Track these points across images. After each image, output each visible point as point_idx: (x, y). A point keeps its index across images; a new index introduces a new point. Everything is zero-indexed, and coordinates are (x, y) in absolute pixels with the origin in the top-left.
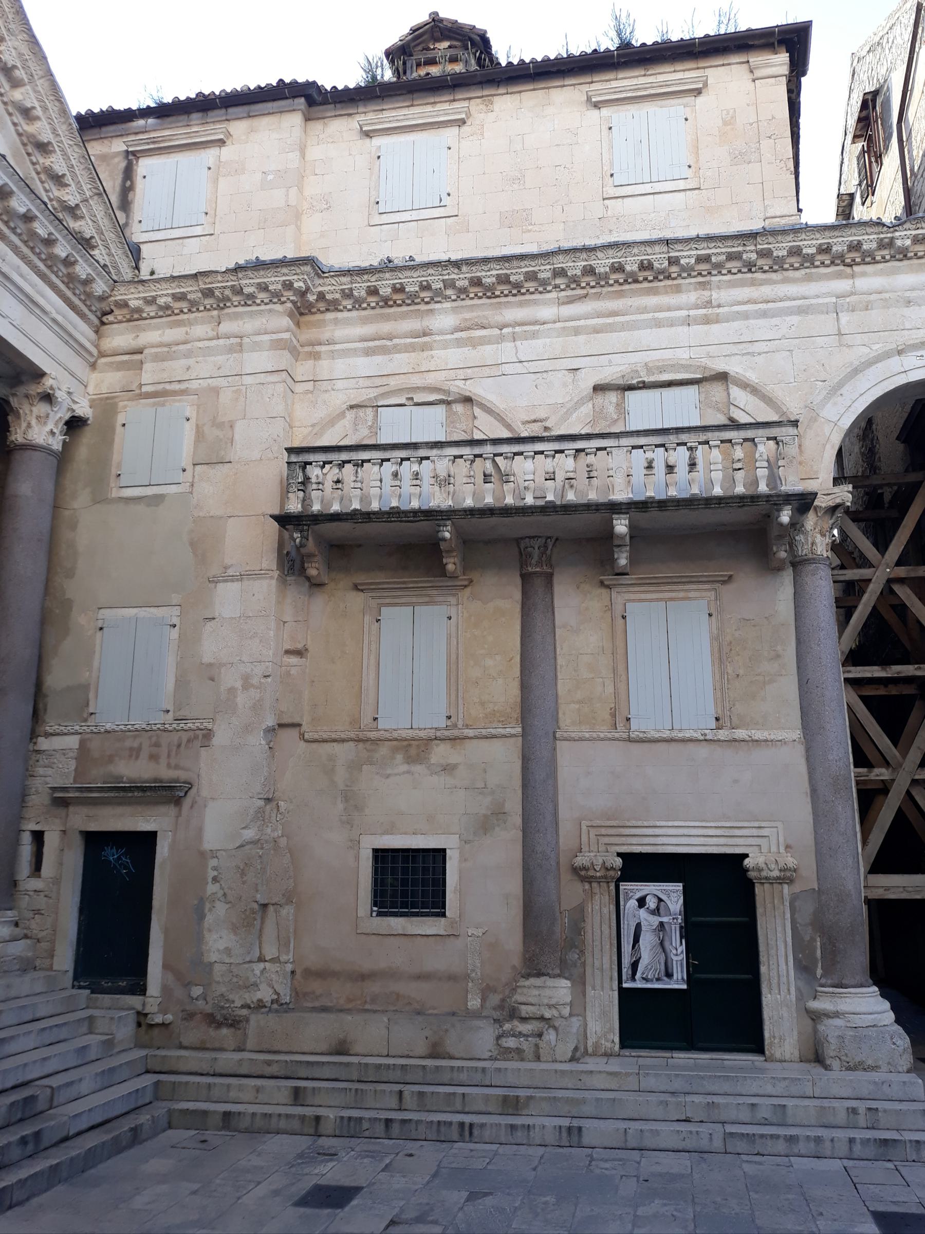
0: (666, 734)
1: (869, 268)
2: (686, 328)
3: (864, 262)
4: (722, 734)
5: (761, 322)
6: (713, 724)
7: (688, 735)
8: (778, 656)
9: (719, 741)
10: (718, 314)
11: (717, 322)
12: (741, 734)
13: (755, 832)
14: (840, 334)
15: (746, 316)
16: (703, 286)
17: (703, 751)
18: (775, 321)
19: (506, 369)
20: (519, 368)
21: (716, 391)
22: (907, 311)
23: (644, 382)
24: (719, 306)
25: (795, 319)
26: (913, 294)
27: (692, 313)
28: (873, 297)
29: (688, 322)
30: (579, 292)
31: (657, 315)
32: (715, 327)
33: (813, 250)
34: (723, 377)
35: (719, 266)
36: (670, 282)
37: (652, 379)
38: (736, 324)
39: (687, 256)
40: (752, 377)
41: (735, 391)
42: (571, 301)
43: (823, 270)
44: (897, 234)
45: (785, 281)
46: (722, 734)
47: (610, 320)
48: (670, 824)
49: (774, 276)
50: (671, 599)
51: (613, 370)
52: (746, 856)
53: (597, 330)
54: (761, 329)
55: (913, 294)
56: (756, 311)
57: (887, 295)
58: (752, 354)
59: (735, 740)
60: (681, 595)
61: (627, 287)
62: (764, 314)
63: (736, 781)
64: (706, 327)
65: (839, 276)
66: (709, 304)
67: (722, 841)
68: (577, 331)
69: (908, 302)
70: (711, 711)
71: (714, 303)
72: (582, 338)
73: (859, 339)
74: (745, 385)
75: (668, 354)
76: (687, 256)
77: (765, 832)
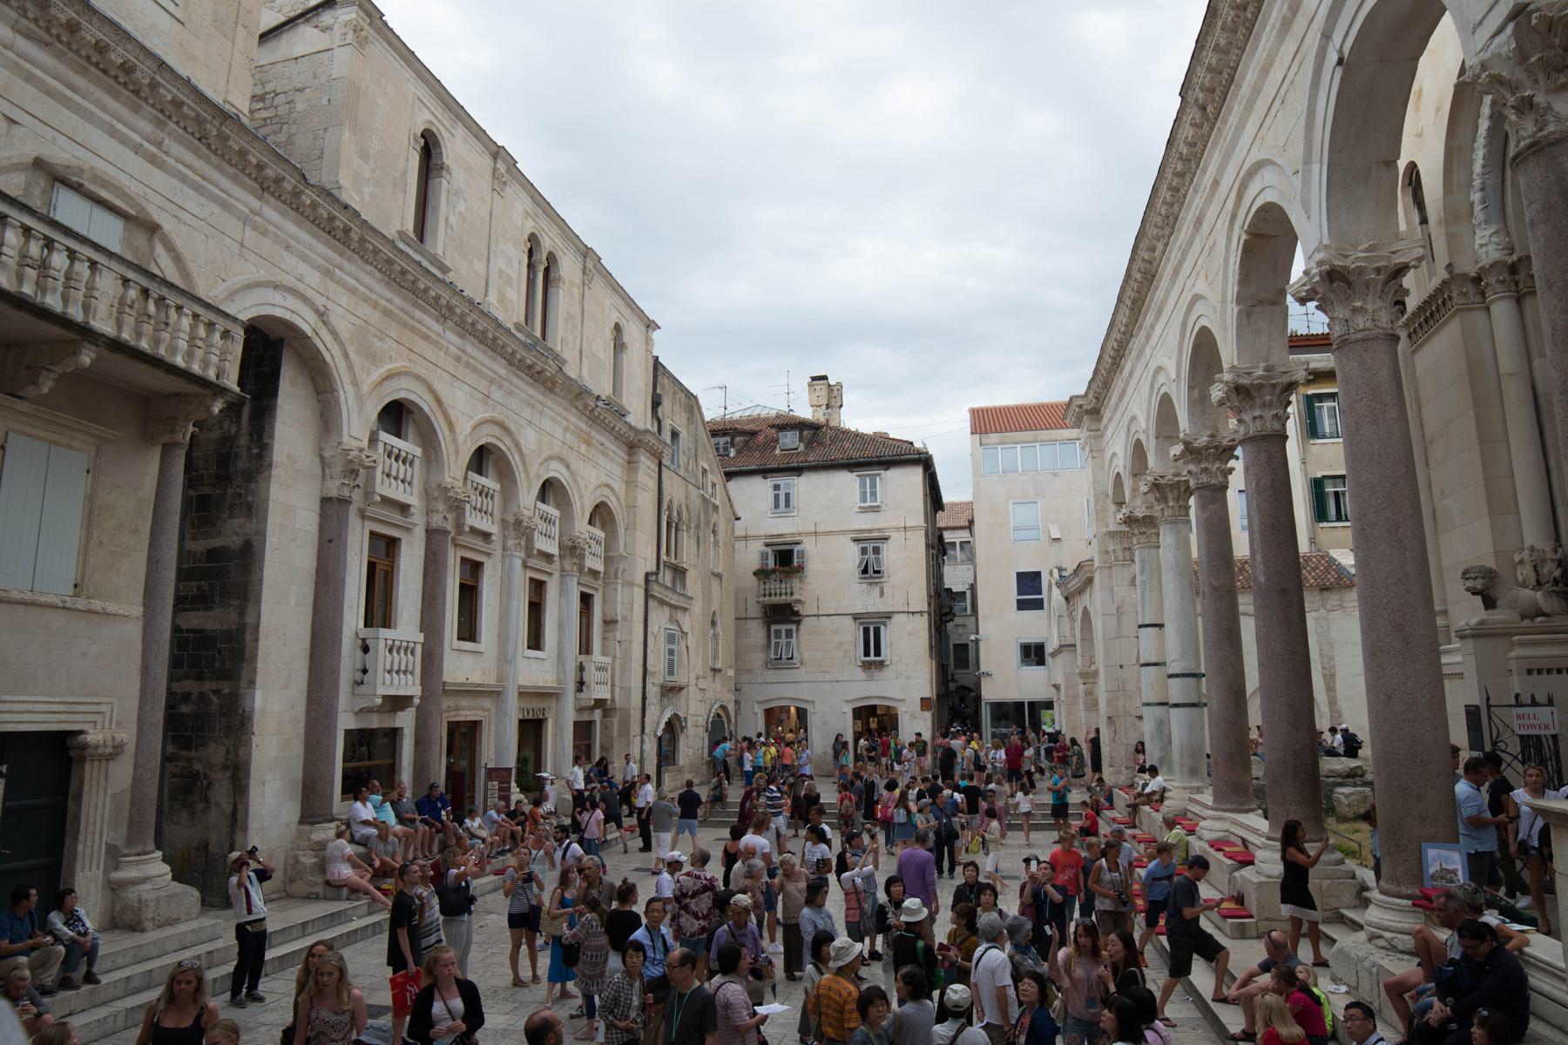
0: (28, 596)
1: (272, 201)
2: (132, 155)
3: (272, 194)
4: (81, 603)
5: (192, 193)
6: (71, 591)
7: (50, 599)
8: (137, 530)
9: (77, 610)
11: (160, 168)
12: (97, 605)
13: (94, 708)
14: (242, 245)
15: (183, 179)
16: (159, 124)
17: (59, 620)
18: (202, 200)
21: (140, 239)
22: (285, 254)
23: (81, 185)
25: (217, 209)
26: (294, 243)
27: (146, 144)
28: (271, 228)
29: (137, 149)
30: (43, 34)
31: (115, 122)
33: (254, 161)
34: (153, 229)
35: (185, 117)
36: (133, 97)
37: (92, 187)
38: (174, 182)
39: (168, 92)
40: (178, 242)
41: (159, 250)
42: (28, 35)
45: (219, 168)
46: (81, 603)
47: (69, 93)
48: (16, 698)
49: (213, 157)
50: (55, 443)
51: (61, 154)
52: (81, 732)
53: (49, 92)
54: (192, 201)
55: (294, 243)
59: (90, 611)
60: (65, 440)
61: (93, 69)
62: (198, 189)
63: (85, 654)
64: (149, 166)
65: (252, 192)
66: (159, 145)
67: (63, 717)
68: (29, 78)
69: (287, 247)
70: (71, 577)
71: (164, 148)
72: (31, 90)
73: (252, 257)
74: (171, 248)
75: (112, 171)
76: (168, 92)
77: (103, 708)
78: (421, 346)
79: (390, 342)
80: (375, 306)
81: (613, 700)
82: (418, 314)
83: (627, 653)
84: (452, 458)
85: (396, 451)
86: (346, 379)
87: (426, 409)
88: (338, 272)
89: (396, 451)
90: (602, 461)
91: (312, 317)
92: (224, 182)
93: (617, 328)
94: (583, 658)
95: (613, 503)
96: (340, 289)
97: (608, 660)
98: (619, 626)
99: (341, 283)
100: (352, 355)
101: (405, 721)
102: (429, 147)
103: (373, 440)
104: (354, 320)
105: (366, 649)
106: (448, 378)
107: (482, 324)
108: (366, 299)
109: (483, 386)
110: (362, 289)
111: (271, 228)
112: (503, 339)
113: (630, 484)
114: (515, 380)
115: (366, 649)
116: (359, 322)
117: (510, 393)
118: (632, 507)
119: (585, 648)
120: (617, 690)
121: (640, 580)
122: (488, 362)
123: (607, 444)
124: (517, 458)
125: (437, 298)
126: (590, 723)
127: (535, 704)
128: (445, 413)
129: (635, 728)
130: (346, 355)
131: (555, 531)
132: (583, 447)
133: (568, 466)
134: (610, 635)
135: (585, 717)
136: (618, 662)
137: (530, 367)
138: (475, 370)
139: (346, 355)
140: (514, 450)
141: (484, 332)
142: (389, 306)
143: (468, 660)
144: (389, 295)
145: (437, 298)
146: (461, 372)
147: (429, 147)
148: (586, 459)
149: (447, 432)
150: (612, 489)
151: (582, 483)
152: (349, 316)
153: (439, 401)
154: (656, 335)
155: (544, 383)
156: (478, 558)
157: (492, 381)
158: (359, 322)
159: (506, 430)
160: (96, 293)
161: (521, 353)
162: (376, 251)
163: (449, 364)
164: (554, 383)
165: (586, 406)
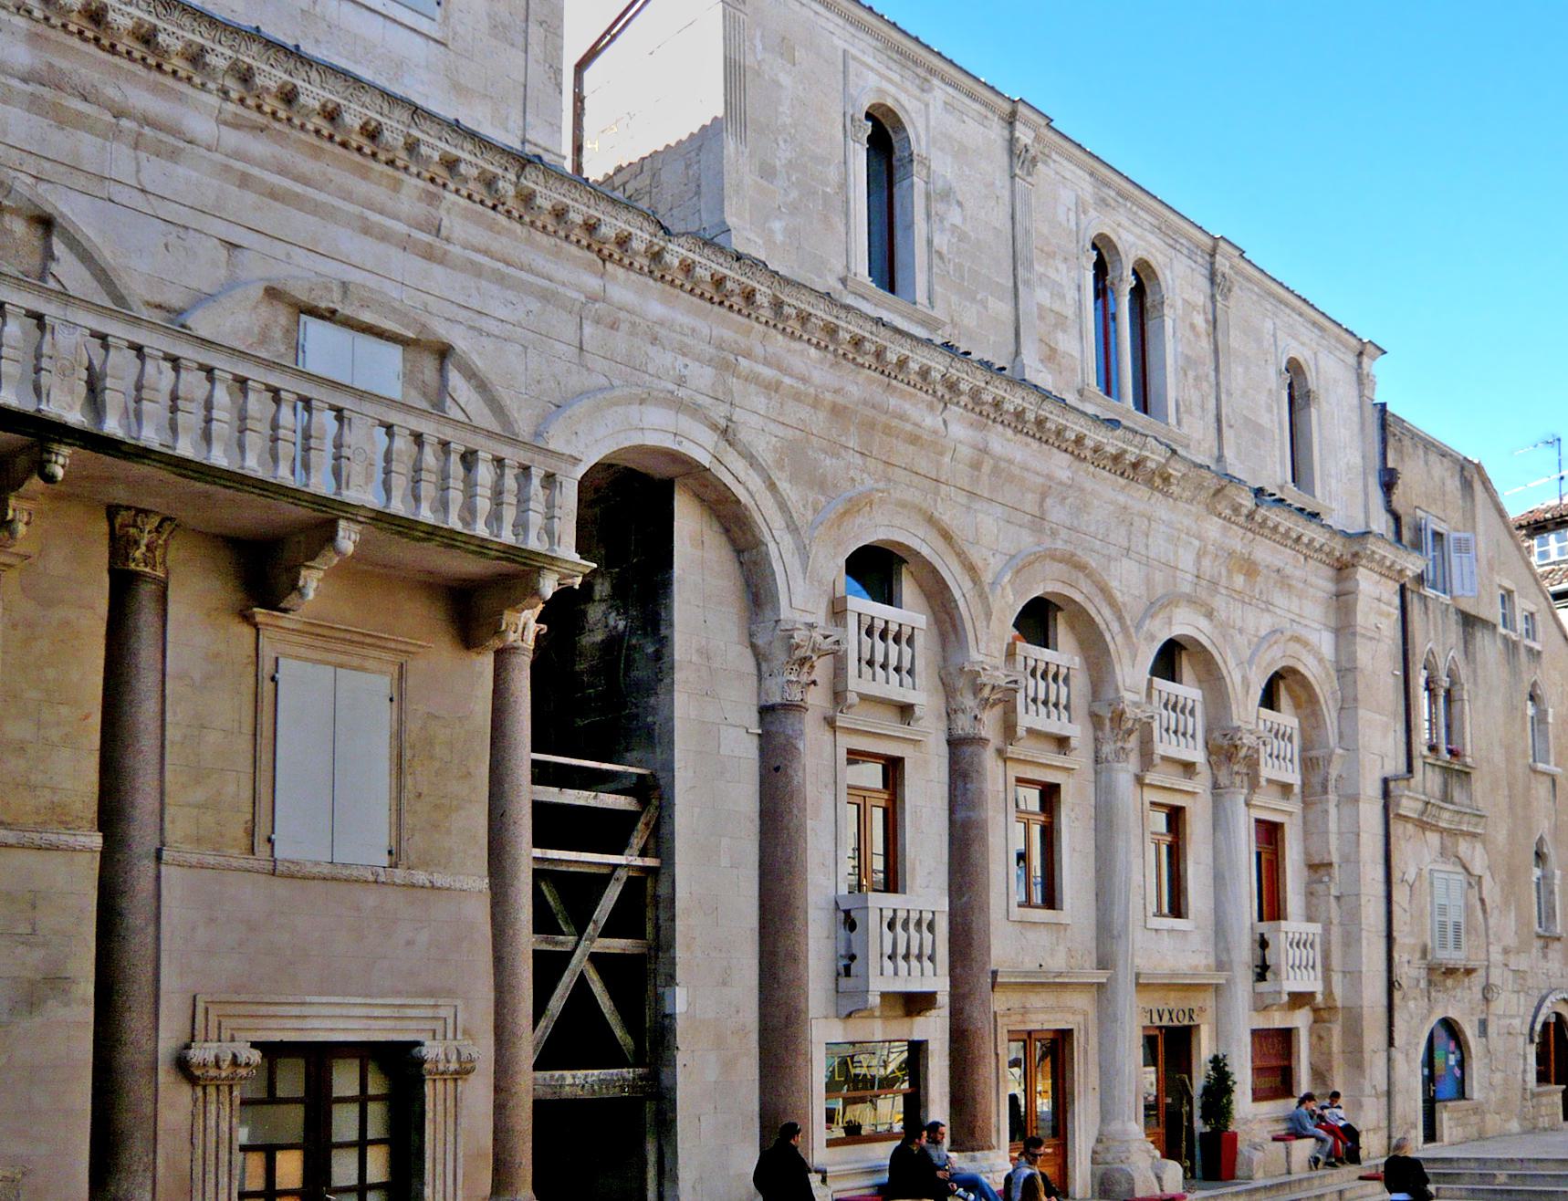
5: (495, 289)
10: (446, 253)
11: (441, 263)
15: (478, 271)
18: (510, 295)
19: (114, 190)
20: (138, 201)
22: (652, 351)
24: (448, 240)
25: (535, 306)
29: (406, 245)
31: (368, 213)
32: (437, 270)
43: (574, 249)
44: (670, 246)
47: (298, 188)
53: (274, 194)
56: (493, 271)
57: (638, 320)
58: (480, 331)
62: (501, 279)
68: (244, 181)
71: (444, 232)
72: (250, 197)
80: (816, 403)
81: (1328, 993)
83: (1352, 918)
84: (981, 624)
85: (879, 625)
86: (778, 522)
87: (925, 551)
89: (879, 625)
90: (1280, 599)
91: (709, 438)
92: (541, 262)
93: (1294, 368)
94: (1265, 927)
95: (1310, 668)
96: (752, 388)
97: (1316, 928)
98: (1336, 871)
100: (784, 486)
101: (933, 1028)
102: (884, 139)
103: (837, 611)
104: (780, 431)
105: (851, 924)
110: (787, 380)
111: (622, 315)
112: (1055, 418)
113: (1344, 628)
115: (851, 924)
116: (790, 433)
118: (1345, 670)
119: (1271, 907)
120: (1337, 978)
121: (1372, 789)
124: (1107, 612)
125: (924, 373)
126: (1285, 1037)
127: (1173, 1001)
128: (961, 556)
129: (1374, 1037)
130: (772, 486)
131: (1198, 724)
133: (1209, 615)
134: (1320, 888)
135: (1277, 1021)
136: (1336, 932)
137: (1116, 458)
139: (772, 486)
140: (1098, 599)
141: (1019, 415)
143: (1040, 938)
145: (924, 373)
147: (884, 139)
148: (1243, 599)
149: (967, 585)
150: (1305, 644)
152: (772, 427)
153: (946, 536)
154: (1377, 368)
155: (1149, 482)
156: (1050, 777)
158: (790, 433)
159: (1081, 567)
160: (345, 452)
162: (804, 318)
164: (1166, 479)
165: (1236, 509)
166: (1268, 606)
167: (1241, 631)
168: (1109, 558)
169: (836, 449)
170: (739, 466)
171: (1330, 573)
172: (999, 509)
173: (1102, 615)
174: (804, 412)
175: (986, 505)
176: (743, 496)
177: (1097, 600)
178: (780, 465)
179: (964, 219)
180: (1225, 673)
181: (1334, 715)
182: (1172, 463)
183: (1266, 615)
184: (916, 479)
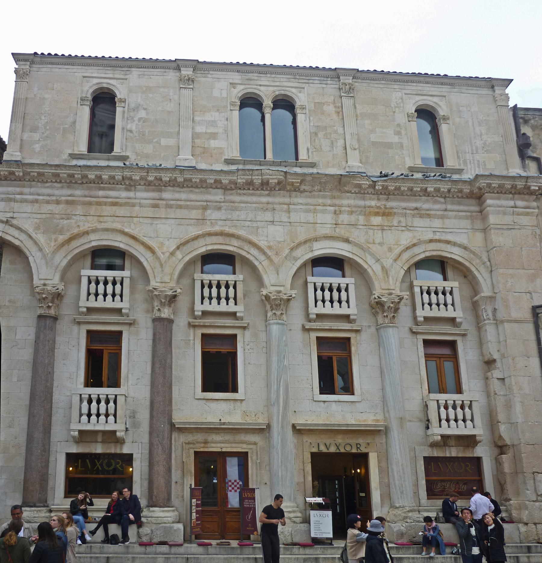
78: (108, 210)
79: (78, 218)
80: (58, 202)
82: (101, 193)
88: (18, 197)
90: (418, 222)
99: (26, 201)
104: (39, 216)
106: (148, 221)
107: (166, 177)
108: (48, 202)
109: (195, 214)
114: (237, 198)
117: (235, 209)
122: (193, 197)
123: (426, 206)
132: (377, 220)
133: (347, 241)
138: (180, 207)
142: (70, 198)
144: (69, 192)
146: (162, 212)
151: (375, 248)
157: (205, 208)
161: (225, 180)
163: (149, 212)
166: (408, 228)
167: (381, 244)
168: (258, 228)
169: (68, 217)
170: (16, 233)
171: (473, 201)
172: (173, 221)
173: (252, 254)
174: (52, 207)
175: (163, 221)
176: (17, 243)
177: (246, 248)
178: (37, 228)
179: (147, 114)
180: (366, 266)
181: (486, 275)
182: (288, 176)
183: (406, 232)
184: (117, 219)
